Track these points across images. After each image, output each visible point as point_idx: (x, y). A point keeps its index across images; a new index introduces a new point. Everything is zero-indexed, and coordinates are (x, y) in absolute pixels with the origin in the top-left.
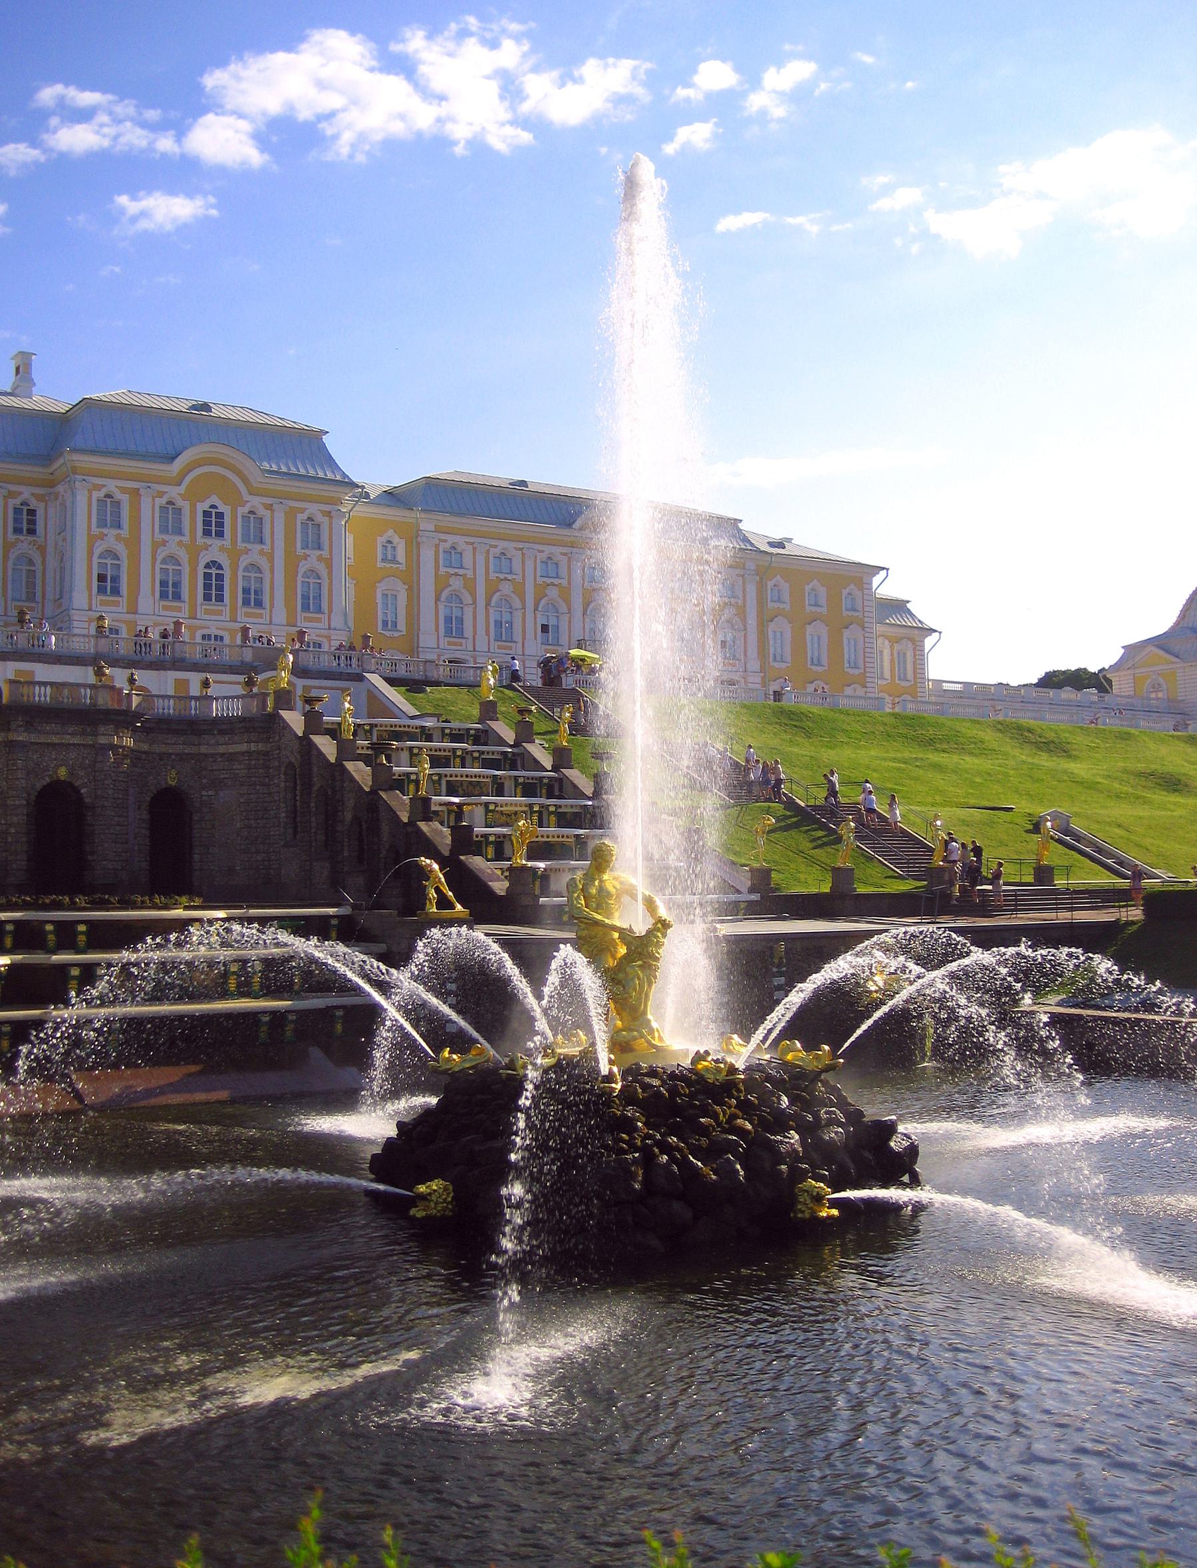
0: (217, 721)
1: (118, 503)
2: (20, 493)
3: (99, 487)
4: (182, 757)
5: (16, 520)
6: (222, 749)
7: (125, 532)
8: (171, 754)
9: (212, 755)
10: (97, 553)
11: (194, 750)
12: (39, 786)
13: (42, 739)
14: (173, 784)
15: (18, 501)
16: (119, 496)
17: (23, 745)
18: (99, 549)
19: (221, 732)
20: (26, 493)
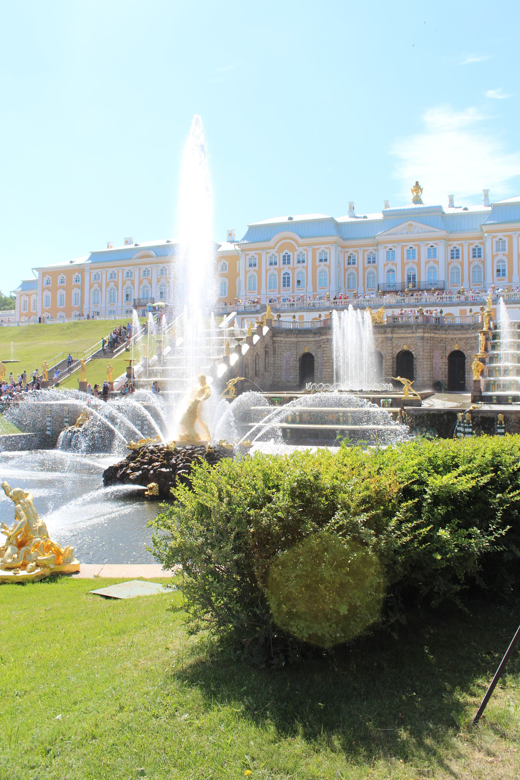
0: (470, 325)
1: (504, 241)
2: (474, 243)
3: (494, 237)
4: (460, 339)
5: (473, 253)
6: (473, 335)
7: (507, 252)
8: (455, 338)
9: (470, 338)
10: (495, 261)
11: (464, 336)
12: (398, 351)
13: (398, 336)
14: (457, 349)
15: (473, 246)
16: (504, 239)
17: (391, 339)
18: (496, 259)
19: (473, 329)
20: (477, 243)
